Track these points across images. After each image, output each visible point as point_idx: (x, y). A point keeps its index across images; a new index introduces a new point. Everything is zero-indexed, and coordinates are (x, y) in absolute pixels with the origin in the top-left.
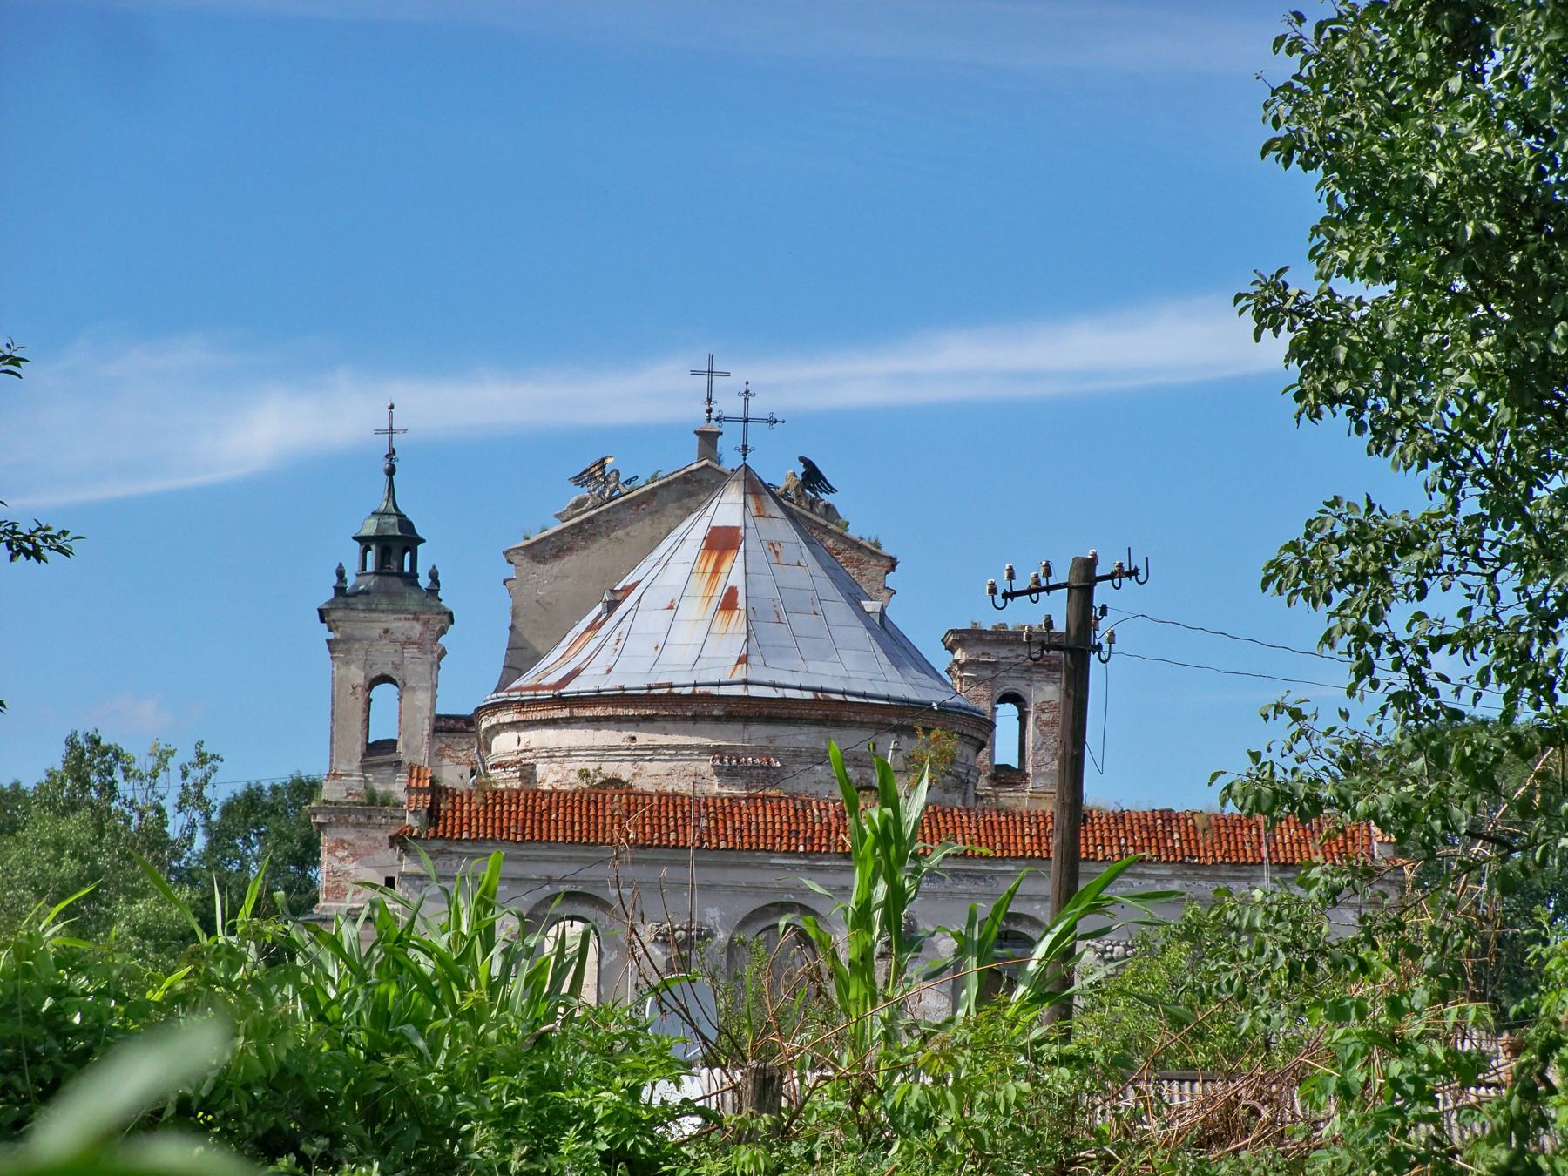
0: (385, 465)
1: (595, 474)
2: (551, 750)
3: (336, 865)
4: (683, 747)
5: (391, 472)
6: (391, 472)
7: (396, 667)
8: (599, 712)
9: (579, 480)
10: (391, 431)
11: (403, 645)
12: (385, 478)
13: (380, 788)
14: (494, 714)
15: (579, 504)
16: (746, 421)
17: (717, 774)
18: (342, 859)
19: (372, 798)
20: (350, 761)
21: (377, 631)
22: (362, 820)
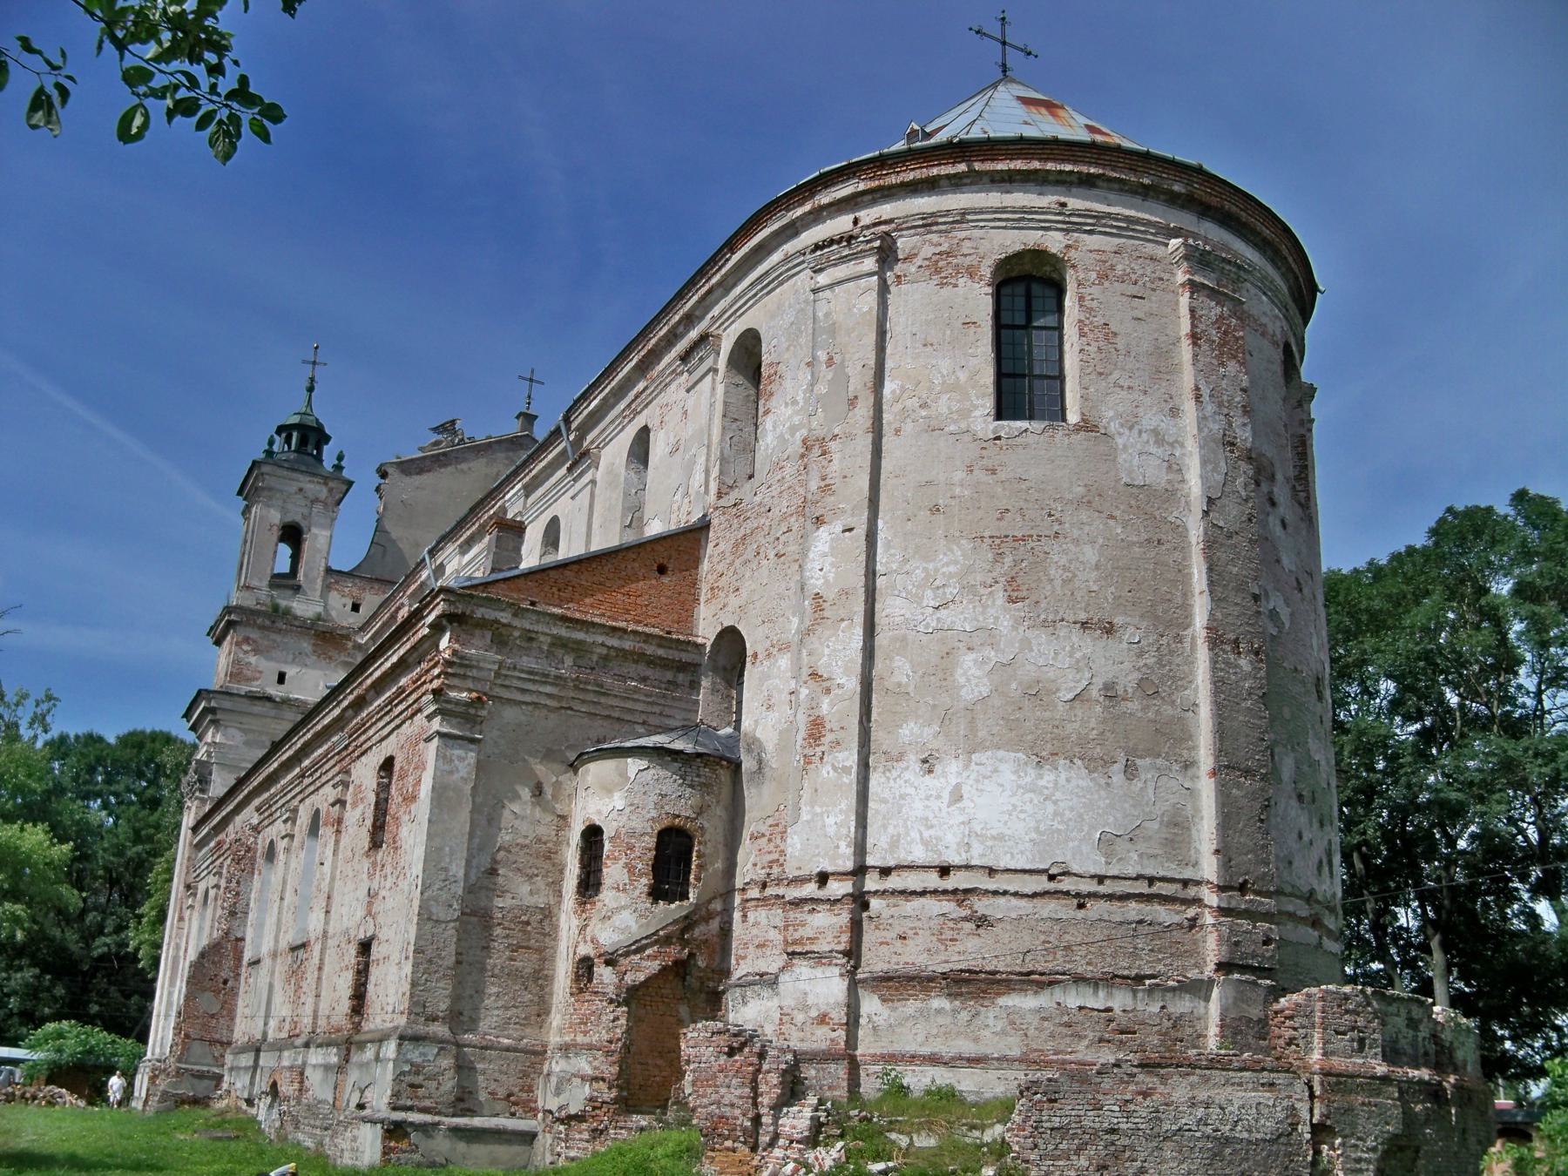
0: (307, 384)
1: (448, 428)
2: (933, 215)
3: (241, 655)
4: (1138, 221)
5: (311, 389)
6: (311, 389)
7: (304, 517)
8: (1018, 165)
9: (435, 430)
10: (314, 363)
11: (312, 502)
12: (305, 394)
13: (283, 603)
14: (812, 195)
15: (437, 443)
16: (1004, 43)
17: (1186, 257)
18: (246, 652)
19: (276, 608)
20: (260, 580)
21: (294, 487)
22: (267, 623)
